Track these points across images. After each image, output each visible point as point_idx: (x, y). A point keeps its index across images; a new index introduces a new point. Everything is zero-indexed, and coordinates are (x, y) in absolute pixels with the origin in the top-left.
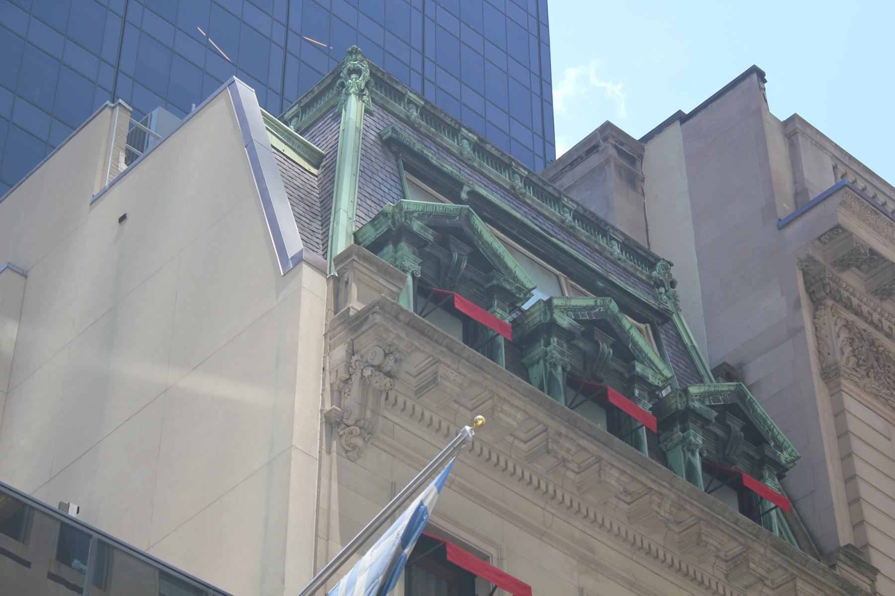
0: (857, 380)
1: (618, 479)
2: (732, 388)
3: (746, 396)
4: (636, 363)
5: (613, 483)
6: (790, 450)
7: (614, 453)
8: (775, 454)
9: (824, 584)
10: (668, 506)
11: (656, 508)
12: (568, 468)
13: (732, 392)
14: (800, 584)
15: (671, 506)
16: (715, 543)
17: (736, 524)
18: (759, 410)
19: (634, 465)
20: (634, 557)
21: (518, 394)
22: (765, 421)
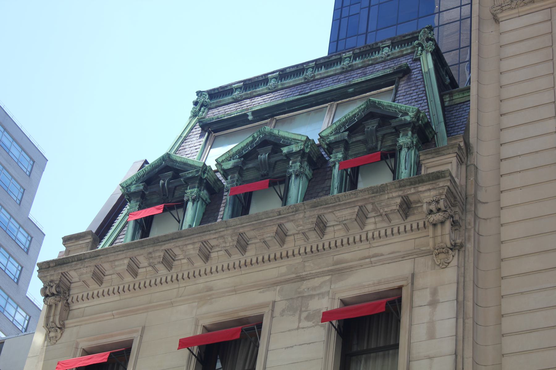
0: (509, 6)
1: (194, 248)
2: (363, 107)
3: (375, 102)
4: (282, 149)
5: (192, 252)
6: (411, 109)
7: (185, 238)
8: (402, 120)
9: (354, 201)
10: (230, 239)
11: (224, 245)
12: (180, 260)
13: (365, 108)
14: (338, 214)
15: (231, 237)
16: (269, 235)
17: (280, 215)
18: (385, 104)
19: (198, 235)
20: (243, 272)
21: (119, 253)
22: (391, 106)
